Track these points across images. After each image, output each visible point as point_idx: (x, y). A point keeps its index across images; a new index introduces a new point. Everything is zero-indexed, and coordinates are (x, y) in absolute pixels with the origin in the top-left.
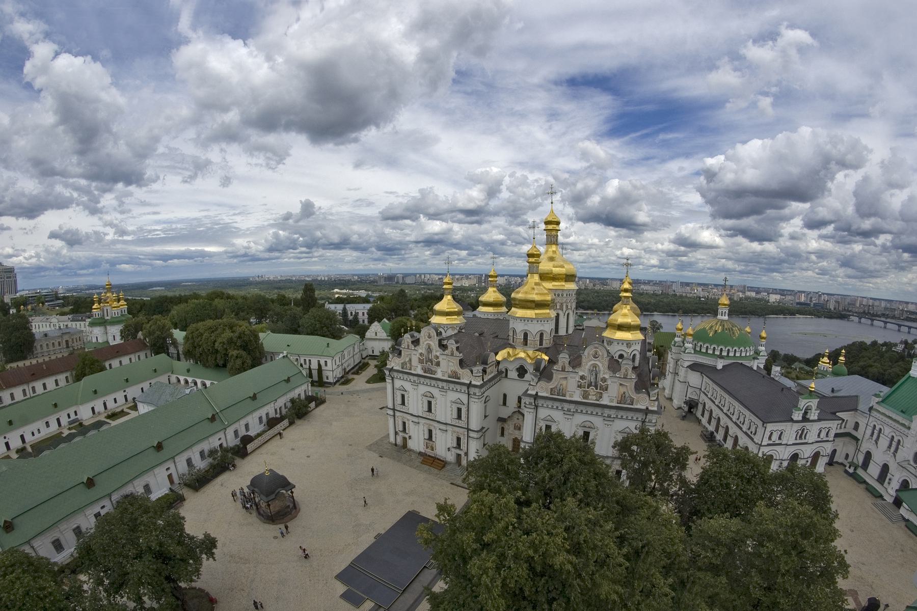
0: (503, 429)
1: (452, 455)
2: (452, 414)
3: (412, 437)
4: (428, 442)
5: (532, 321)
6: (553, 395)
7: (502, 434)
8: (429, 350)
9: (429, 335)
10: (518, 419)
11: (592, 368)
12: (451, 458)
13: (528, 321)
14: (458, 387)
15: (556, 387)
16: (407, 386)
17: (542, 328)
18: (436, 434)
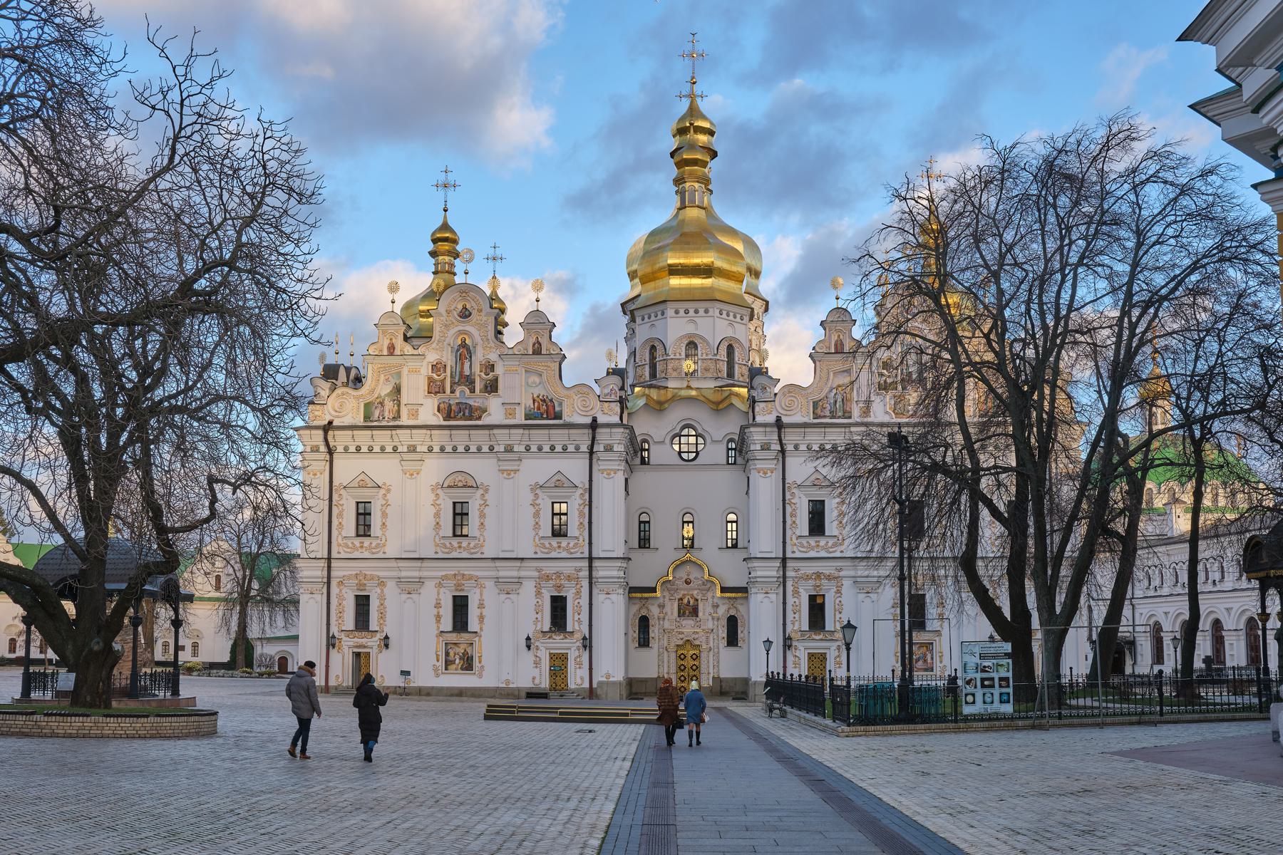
0: (644, 623)
1: (537, 664)
2: (537, 526)
3: (392, 642)
4: (453, 637)
5: (706, 311)
6: (820, 417)
7: (644, 642)
8: (464, 351)
9: (465, 308)
10: (688, 582)
12: (536, 672)
13: (696, 312)
14: (559, 437)
16: (383, 469)
17: (730, 333)
18: (481, 606)
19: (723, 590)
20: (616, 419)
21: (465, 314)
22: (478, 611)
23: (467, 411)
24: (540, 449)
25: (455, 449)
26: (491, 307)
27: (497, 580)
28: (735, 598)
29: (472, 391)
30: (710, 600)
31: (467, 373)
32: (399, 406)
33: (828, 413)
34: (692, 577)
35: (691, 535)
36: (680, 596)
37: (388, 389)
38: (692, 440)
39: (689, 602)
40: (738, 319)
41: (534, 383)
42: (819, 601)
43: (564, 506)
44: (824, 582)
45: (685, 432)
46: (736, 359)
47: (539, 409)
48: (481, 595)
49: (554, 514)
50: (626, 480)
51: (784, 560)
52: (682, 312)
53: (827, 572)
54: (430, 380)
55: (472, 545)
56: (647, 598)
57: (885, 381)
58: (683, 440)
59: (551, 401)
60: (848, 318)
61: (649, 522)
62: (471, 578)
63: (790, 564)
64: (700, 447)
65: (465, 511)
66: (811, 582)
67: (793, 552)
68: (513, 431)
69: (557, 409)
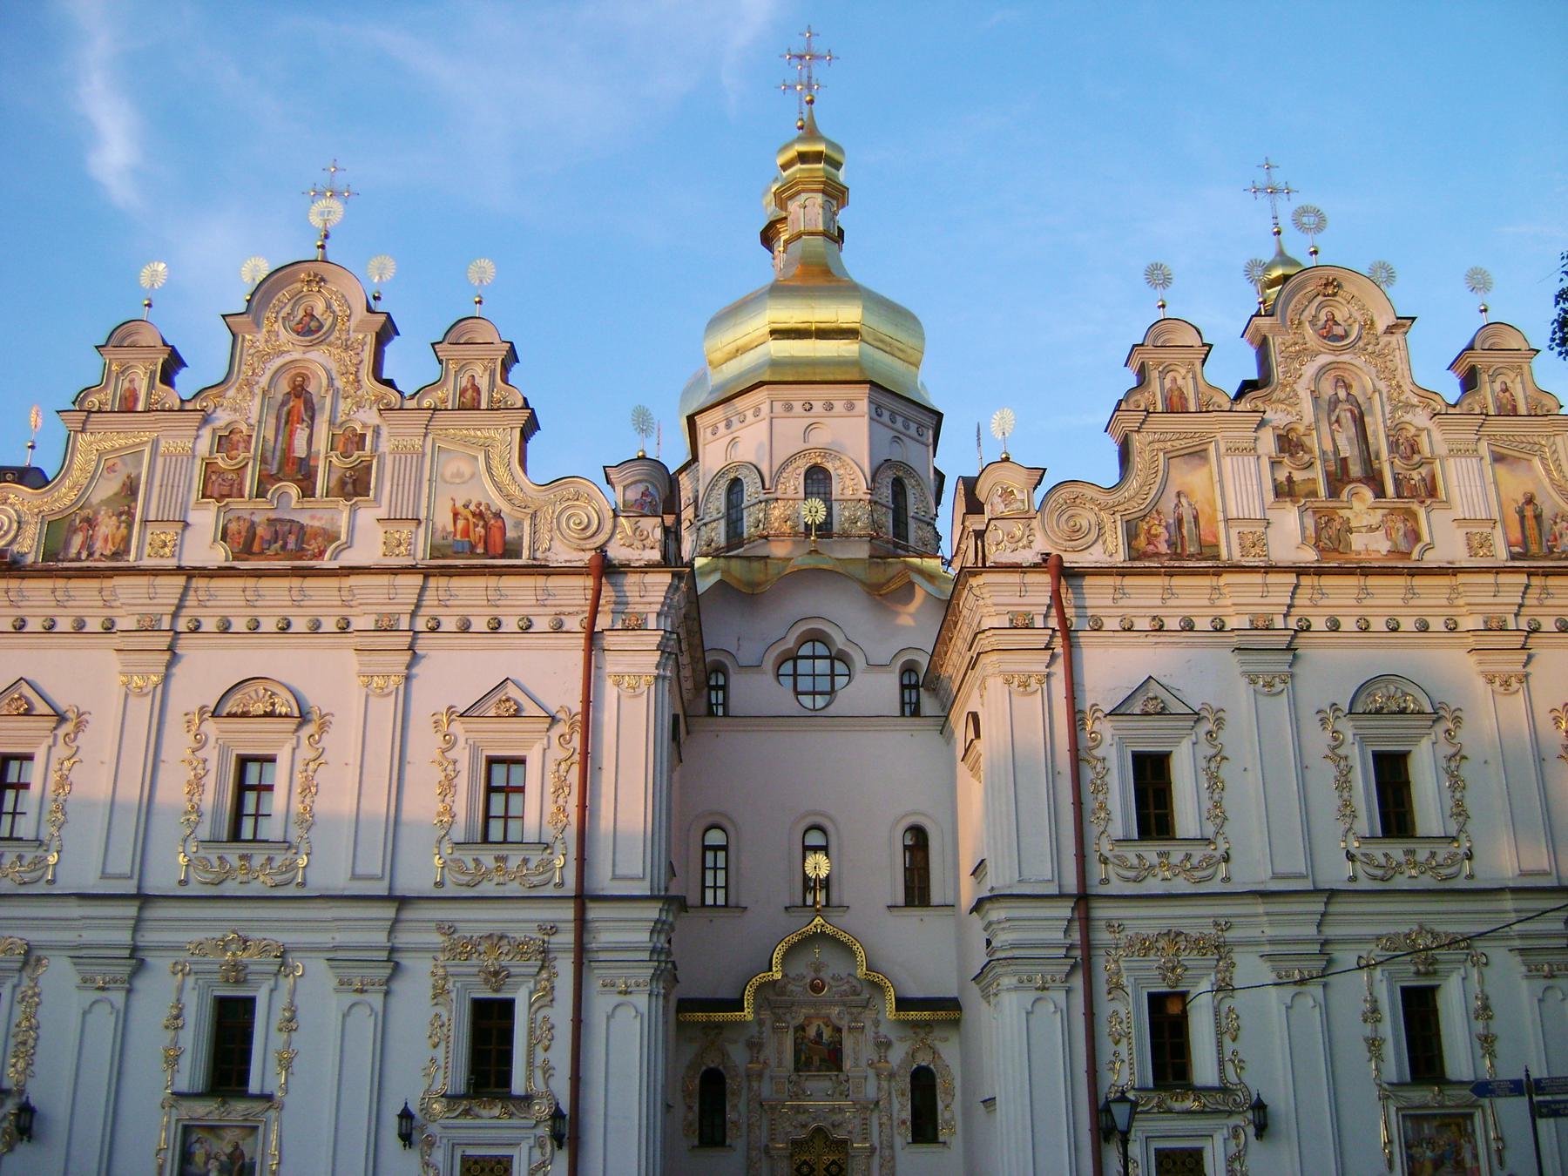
5: (850, 406)
10: (816, 988)
11: (1327, 389)
13: (829, 407)
15: (1155, 506)
18: (290, 1024)
19: (903, 1004)
20: (656, 555)
21: (309, 329)
22: (278, 1039)
23: (292, 540)
24: (465, 628)
25: (254, 627)
26: (370, 310)
27: (336, 957)
28: (928, 1025)
29: (307, 491)
30: (870, 1031)
31: (300, 450)
32: (130, 526)
33: (1163, 548)
34: (826, 975)
35: (823, 874)
36: (800, 1020)
37: (108, 488)
38: (822, 666)
39: (820, 1034)
40: (913, 431)
41: (459, 474)
42: (1173, 1008)
43: (515, 769)
44: (1189, 958)
45: (806, 650)
46: (911, 510)
47: (466, 533)
48: (293, 992)
49: (490, 789)
50: (676, 718)
51: (1083, 899)
52: (798, 407)
53: (1194, 933)
54: (209, 464)
55: (279, 860)
56: (719, 1027)
57: (1290, 479)
58: (804, 666)
59: (498, 515)
60: (1196, 342)
61: (725, 848)
62: (263, 951)
63: (1101, 912)
64: (840, 681)
65: (266, 781)
66: (1154, 961)
67: (1105, 881)
68: (402, 580)
69: (511, 534)
